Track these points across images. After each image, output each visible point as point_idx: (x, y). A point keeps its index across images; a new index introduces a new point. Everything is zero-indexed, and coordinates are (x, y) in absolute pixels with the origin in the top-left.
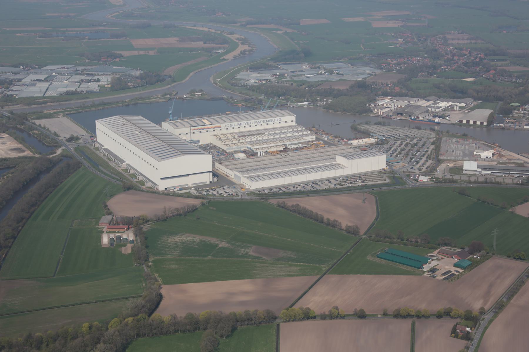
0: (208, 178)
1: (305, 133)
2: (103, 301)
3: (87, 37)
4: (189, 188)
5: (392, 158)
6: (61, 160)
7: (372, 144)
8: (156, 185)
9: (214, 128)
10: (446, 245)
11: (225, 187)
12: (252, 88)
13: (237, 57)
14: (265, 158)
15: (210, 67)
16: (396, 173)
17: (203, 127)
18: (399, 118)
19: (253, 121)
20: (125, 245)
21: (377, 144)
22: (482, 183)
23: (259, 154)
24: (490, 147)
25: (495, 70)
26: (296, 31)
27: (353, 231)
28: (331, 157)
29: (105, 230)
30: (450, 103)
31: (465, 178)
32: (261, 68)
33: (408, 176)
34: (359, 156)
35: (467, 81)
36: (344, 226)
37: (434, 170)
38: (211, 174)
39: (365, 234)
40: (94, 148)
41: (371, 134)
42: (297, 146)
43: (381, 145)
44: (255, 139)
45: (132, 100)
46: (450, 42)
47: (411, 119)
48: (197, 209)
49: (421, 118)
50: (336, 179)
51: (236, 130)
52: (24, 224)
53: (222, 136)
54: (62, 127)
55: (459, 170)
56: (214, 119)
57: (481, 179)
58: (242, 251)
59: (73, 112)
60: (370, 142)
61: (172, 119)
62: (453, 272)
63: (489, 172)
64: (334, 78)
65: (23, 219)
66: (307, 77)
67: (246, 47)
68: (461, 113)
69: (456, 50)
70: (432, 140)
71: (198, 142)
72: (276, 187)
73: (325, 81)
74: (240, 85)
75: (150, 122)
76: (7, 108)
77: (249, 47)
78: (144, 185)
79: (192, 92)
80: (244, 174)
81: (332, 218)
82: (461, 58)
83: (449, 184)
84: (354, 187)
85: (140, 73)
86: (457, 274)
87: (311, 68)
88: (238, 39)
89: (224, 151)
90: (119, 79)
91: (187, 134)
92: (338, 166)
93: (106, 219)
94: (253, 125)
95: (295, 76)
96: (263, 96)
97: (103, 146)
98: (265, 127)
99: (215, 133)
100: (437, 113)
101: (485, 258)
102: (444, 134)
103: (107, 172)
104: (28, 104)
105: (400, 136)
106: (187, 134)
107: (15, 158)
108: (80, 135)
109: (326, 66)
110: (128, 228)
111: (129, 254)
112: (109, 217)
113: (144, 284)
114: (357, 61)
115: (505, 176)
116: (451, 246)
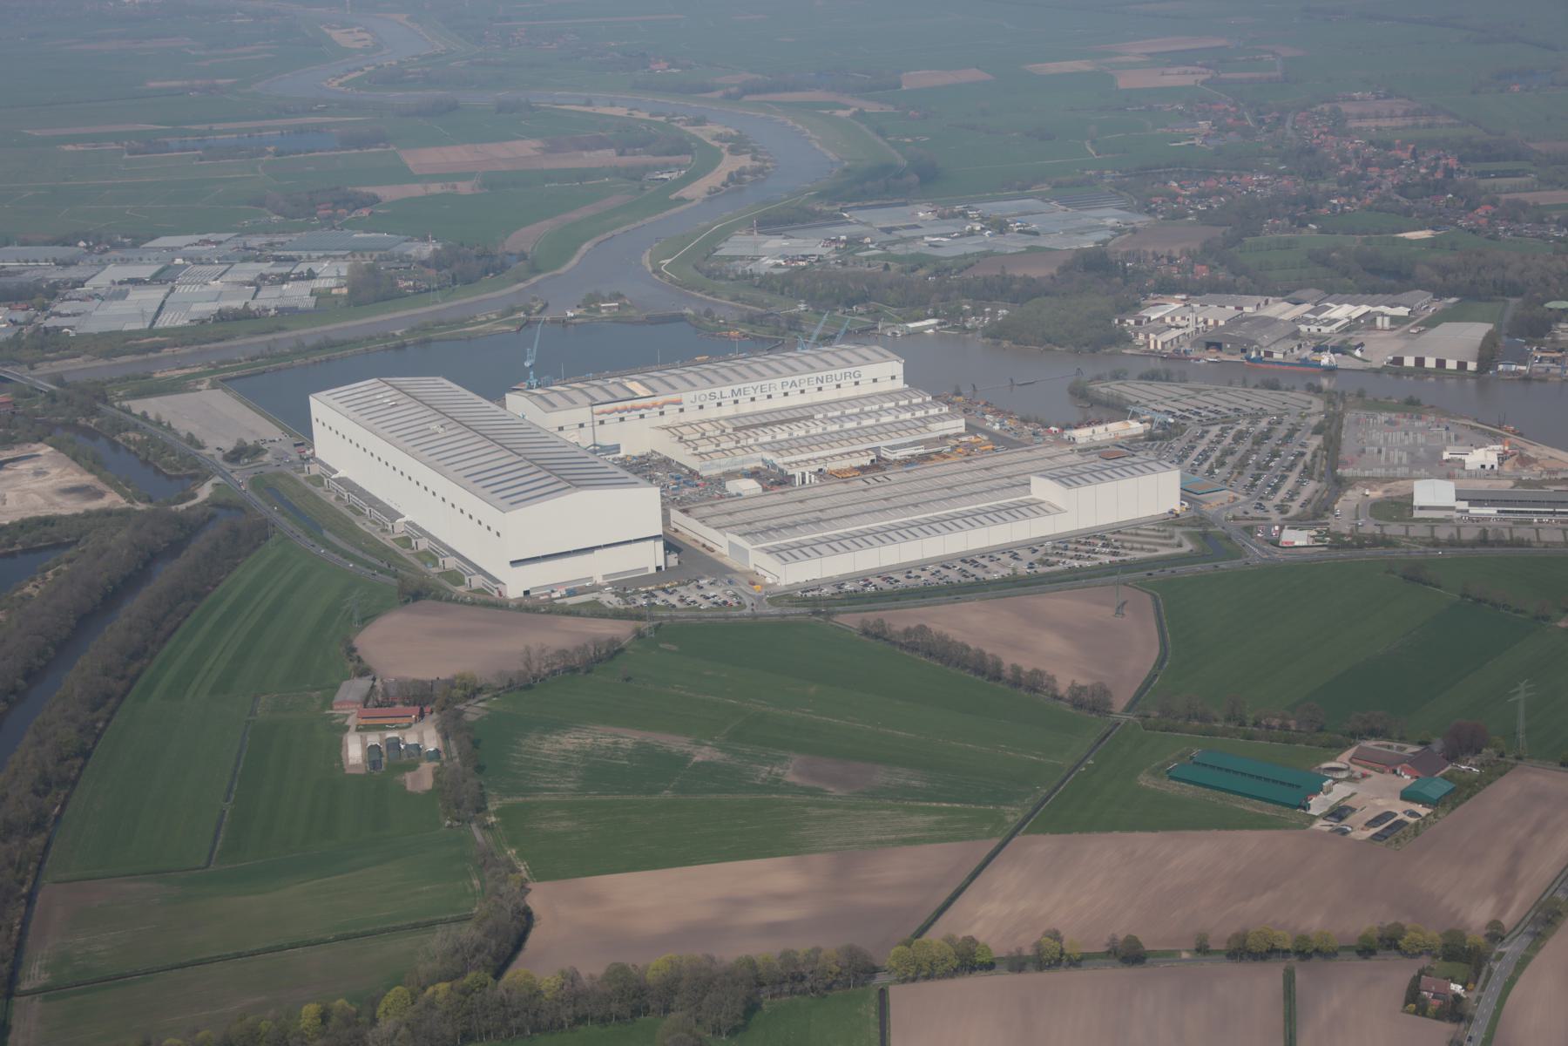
0: (651, 557)
1: (933, 411)
2: (356, 936)
3: (271, 149)
4: (596, 588)
5: (1196, 477)
6: (212, 518)
7: (1134, 439)
8: (499, 582)
10: (1373, 733)
11: (702, 582)
12: (767, 283)
13: (718, 190)
14: (818, 491)
15: (639, 223)
16: (1212, 524)
17: (629, 404)
18: (1211, 356)
19: (778, 382)
20: (413, 767)
21: (1150, 437)
22: (1473, 544)
23: (798, 481)
24: (1491, 434)
25: (1494, 203)
26: (890, 109)
27: (1091, 703)
28: (1013, 481)
29: (352, 721)
30: (1364, 309)
31: (1419, 531)
32: (792, 222)
33: (1249, 530)
34: (1098, 475)
35: (1411, 241)
36: (1063, 683)
37: (1327, 509)
38: (660, 545)
39: (1128, 709)
40: (307, 479)
41: (1131, 408)
42: (911, 451)
43: (1163, 440)
44: (786, 436)
45: (413, 329)
46: (1353, 124)
47: (1248, 359)
48: (621, 650)
49: (1278, 356)
50: (1032, 546)
51: (728, 410)
52: (113, 713)
53: (684, 430)
54: (211, 418)
55: (1401, 507)
56: (660, 379)
57: (1470, 534)
58: (764, 771)
59: (240, 373)
60: (1129, 433)
61: (534, 382)
62: (1400, 816)
63: (1492, 511)
64: (1012, 244)
65: (108, 697)
66: (931, 245)
67: (745, 161)
68: (1398, 337)
69: (1372, 149)
70: (1314, 421)
71: (617, 448)
72: (854, 577)
73: (985, 255)
74: (732, 276)
75: (470, 395)
76: (44, 368)
77: (754, 159)
78: (462, 583)
79: (591, 301)
80: (757, 542)
81: (1027, 666)
82: (1388, 172)
83: (1373, 551)
84: (1087, 569)
85: (435, 250)
86: (1412, 820)
87: (942, 217)
88: (718, 137)
89: (693, 473)
90: (371, 270)
91: (581, 426)
92: (1036, 508)
93: (355, 688)
94: (777, 393)
95: (894, 243)
96: (802, 307)
98: (812, 397)
99: (666, 421)
100: (1326, 338)
101: (1495, 771)
102: (1350, 400)
103: (351, 550)
104: (110, 354)
105: (1217, 412)
106: (581, 426)
107: (76, 516)
108: (264, 441)
109: (988, 208)
110: (422, 715)
111: (429, 792)
112: (364, 684)
113: (476, 882)
114: (1076, 191)
115: (1540, 521)
116: (1389, 737)
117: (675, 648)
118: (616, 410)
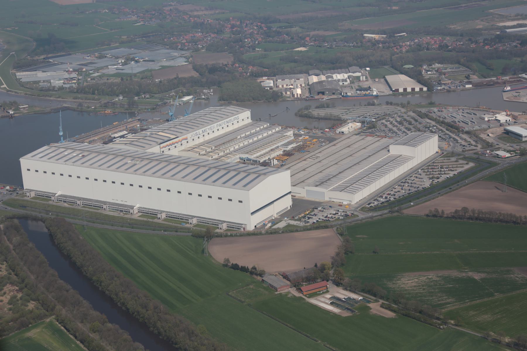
9: (181, 142)
19: (215, 125)
35: (301, 51)
47: (343, 96)
51: (201, 140)
97: (56, 194)
99: (183, 148)
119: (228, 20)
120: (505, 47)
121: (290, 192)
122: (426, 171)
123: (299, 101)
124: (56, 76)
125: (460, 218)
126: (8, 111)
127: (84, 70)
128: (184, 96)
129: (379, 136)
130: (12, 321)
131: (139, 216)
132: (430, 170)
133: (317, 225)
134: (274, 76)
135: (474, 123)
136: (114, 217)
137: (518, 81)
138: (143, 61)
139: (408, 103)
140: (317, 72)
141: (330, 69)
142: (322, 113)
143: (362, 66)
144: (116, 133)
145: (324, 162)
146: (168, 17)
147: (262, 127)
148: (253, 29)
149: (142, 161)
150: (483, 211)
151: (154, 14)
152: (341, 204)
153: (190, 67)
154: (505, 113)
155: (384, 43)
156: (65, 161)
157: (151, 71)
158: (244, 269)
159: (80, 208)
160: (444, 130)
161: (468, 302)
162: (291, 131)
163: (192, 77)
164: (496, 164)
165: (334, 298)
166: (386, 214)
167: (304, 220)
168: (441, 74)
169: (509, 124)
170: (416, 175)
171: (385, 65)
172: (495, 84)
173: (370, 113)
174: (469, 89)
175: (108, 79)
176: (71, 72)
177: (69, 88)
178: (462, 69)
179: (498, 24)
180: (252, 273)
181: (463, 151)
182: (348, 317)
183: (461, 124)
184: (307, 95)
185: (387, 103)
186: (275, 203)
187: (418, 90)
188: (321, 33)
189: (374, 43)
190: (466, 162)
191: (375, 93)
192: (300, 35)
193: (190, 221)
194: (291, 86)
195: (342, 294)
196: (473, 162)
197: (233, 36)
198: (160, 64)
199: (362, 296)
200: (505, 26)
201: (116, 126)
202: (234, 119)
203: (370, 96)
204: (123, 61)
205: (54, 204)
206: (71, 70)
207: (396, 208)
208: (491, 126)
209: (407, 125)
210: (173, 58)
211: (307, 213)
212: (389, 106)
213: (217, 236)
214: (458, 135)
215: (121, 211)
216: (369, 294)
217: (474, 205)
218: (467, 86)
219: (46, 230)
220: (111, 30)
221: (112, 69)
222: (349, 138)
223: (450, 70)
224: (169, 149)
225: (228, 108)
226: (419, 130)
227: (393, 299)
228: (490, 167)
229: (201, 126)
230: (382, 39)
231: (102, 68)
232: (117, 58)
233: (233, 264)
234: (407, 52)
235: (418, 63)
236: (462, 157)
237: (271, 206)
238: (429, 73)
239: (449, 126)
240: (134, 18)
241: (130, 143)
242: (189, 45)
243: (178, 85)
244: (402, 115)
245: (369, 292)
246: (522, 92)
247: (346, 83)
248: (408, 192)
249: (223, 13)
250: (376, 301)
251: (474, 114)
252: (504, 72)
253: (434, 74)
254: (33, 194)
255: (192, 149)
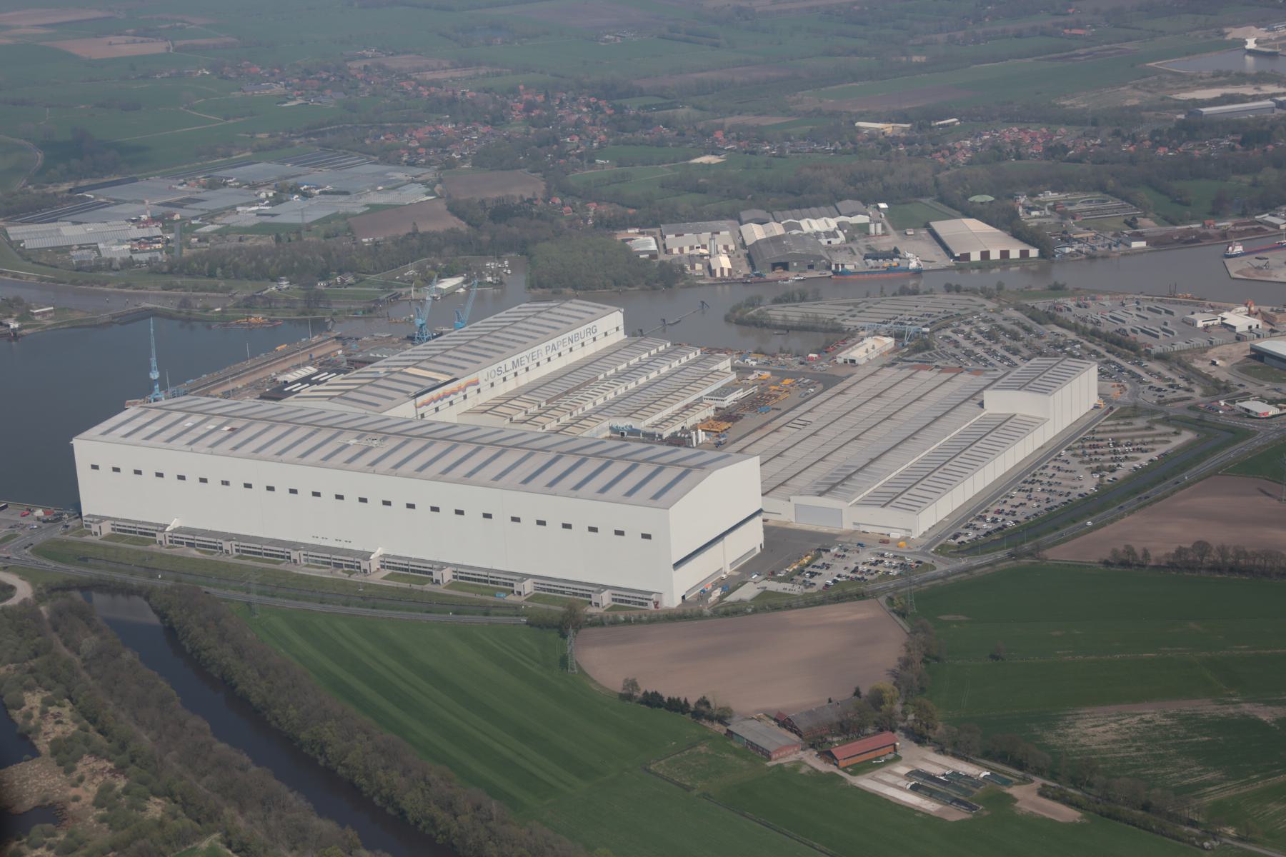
8: (652, 593)
9: (464, 390)
19: (543, 346)
51: (511, 385)
97: (167, 526)
99: (469, 405)
117: (961, 618)
118: (434, 400)
119: (514, 91)
120: (1205, 151)
121: (760, 511)
122: (1080, 452)
123: (727, 287)
124: (112, 232)
125: (1188, 568)
126: (5, 321)
127: (177, 217)
128: (440, 277)
129: (944, 370)
130: (114, 849)
131: (385, 578)
132: (1088, 451)
133: (840, 591)
134: (656, 225)
135: (1172, 333)
136: (322, 580)
137: (1259, 231)
138: (320, 193)
139: (1000, 287)
140: (761, 214)
141: (791, 207)
142: (794, 313)
143: (868, 200)
144: (287, 371)
145: (827, 434)
146: (362, 85)
147: (653, 352)
148: (580, 111)
149: (384, 439)
150: (1248, 550)
151: (328, 79)
152: (886, 538)
153: (441, 206)
154: (1243, 309)
155: (908, 142)
156: (190, 443)
157: (345, 217)
158: (676, 706)
159: (230, 559)
160: (1103, 351)
161: (1257, 780)
162: (722, 359)
163: (452, 231)
164: (1248, 434)
165: (916, 773)
166: (1002, 560)
167: (800, 579)
168: (1064, 215)
169: (1258, 336)
170: (1058, 464)
171: (922, 196)
172: (1199, 239)
173: (913, 311)
174: (1139, 252)
175: (240, 240)
176: (145, 222)
177: (148, 263)
178: (1113, 203)
179: (1175, 96)
180: (697, 715)
181: (1159, 403)
182: (963, 821)
183: (1141, 338)
184: (745, 270)
185: (949, 289)
186: (727, 538)
187: (1018, 256)
188: (750, 120)
189: (887, 144)
190: (1173, 430)
191: (913, 265)
192: (701, 126)
193: (517, 587)
194: (701, 251)
195: (938, 764)
196: (1190, 429)
197: (533, 130)
198: (364, 200)
199: (988, 768)
200: (1194, 100)
201: (285, 355)
202: (586, 333)
203: (901, 270)
204: (271, 194)
205: (165, 550)
206: (144, 217)
207: (1027, 546)
208: (1216, 340)
209: (1009, 343)
210: (395, 186)
211: (806, 561)
212: (954, 296)
213: (593, 624)
214: (1139, 364)
215: (339, 566)
216: (1003, 763)
217: (1219, 536)
218: (1135, 245)
219: (154, 619)
220: (227, 118)
221: (247, 215)
222: (873, 374)
223: (1084, 207)
224: (437, 409)
225: (567, 305)
226: (1040, 354)
227: (1069, 775)
228: (1236, 442)
229: (509, 351)
230: (903, 134)
231: (221, 212)
232: (254, 186)
233: (646, 693)
234: (970, 163)
235: (1004, 188)
236: (1160, 417)
237: (719, 545)
238: (1034, 213)
239: (1111, 342)
240: (279, 89)
241: (339, 396)
242: (427, 154)
243: (420, 251)
244: (990, 316)
245: (1003, 758)
246: (1274, 258)
247: (835, 242)
248: (1044, 505)
249: (498, 75)
250: (1025, 781)
251: (1167, 312)
252: (1217, 210)
253: (1046, 217)
254: (106, 529)
255: (490, 409)
